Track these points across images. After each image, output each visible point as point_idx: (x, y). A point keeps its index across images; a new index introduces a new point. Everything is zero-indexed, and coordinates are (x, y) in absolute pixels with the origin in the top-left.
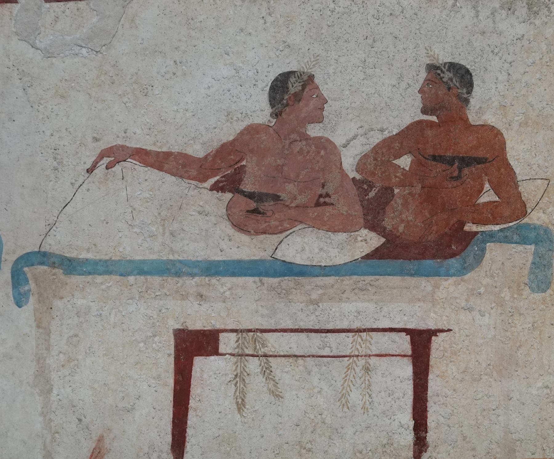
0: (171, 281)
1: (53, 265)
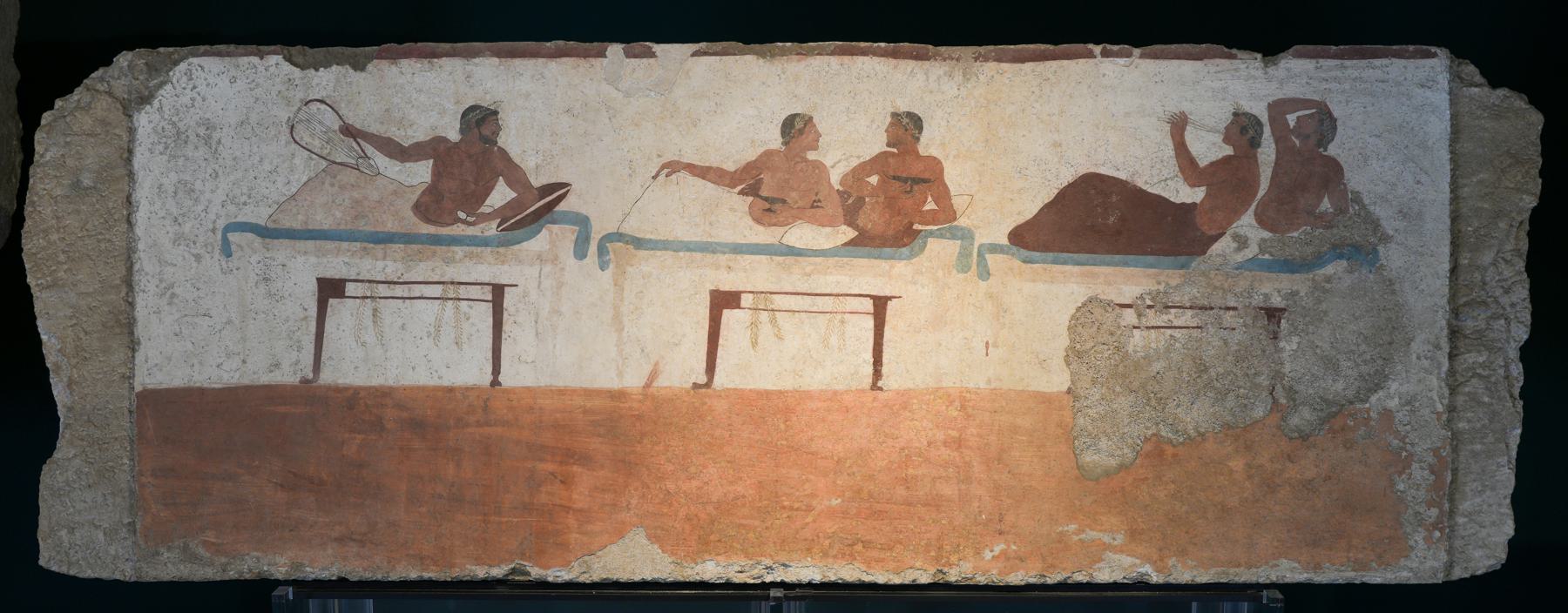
0: (709, 258)
1: (627, 243)
